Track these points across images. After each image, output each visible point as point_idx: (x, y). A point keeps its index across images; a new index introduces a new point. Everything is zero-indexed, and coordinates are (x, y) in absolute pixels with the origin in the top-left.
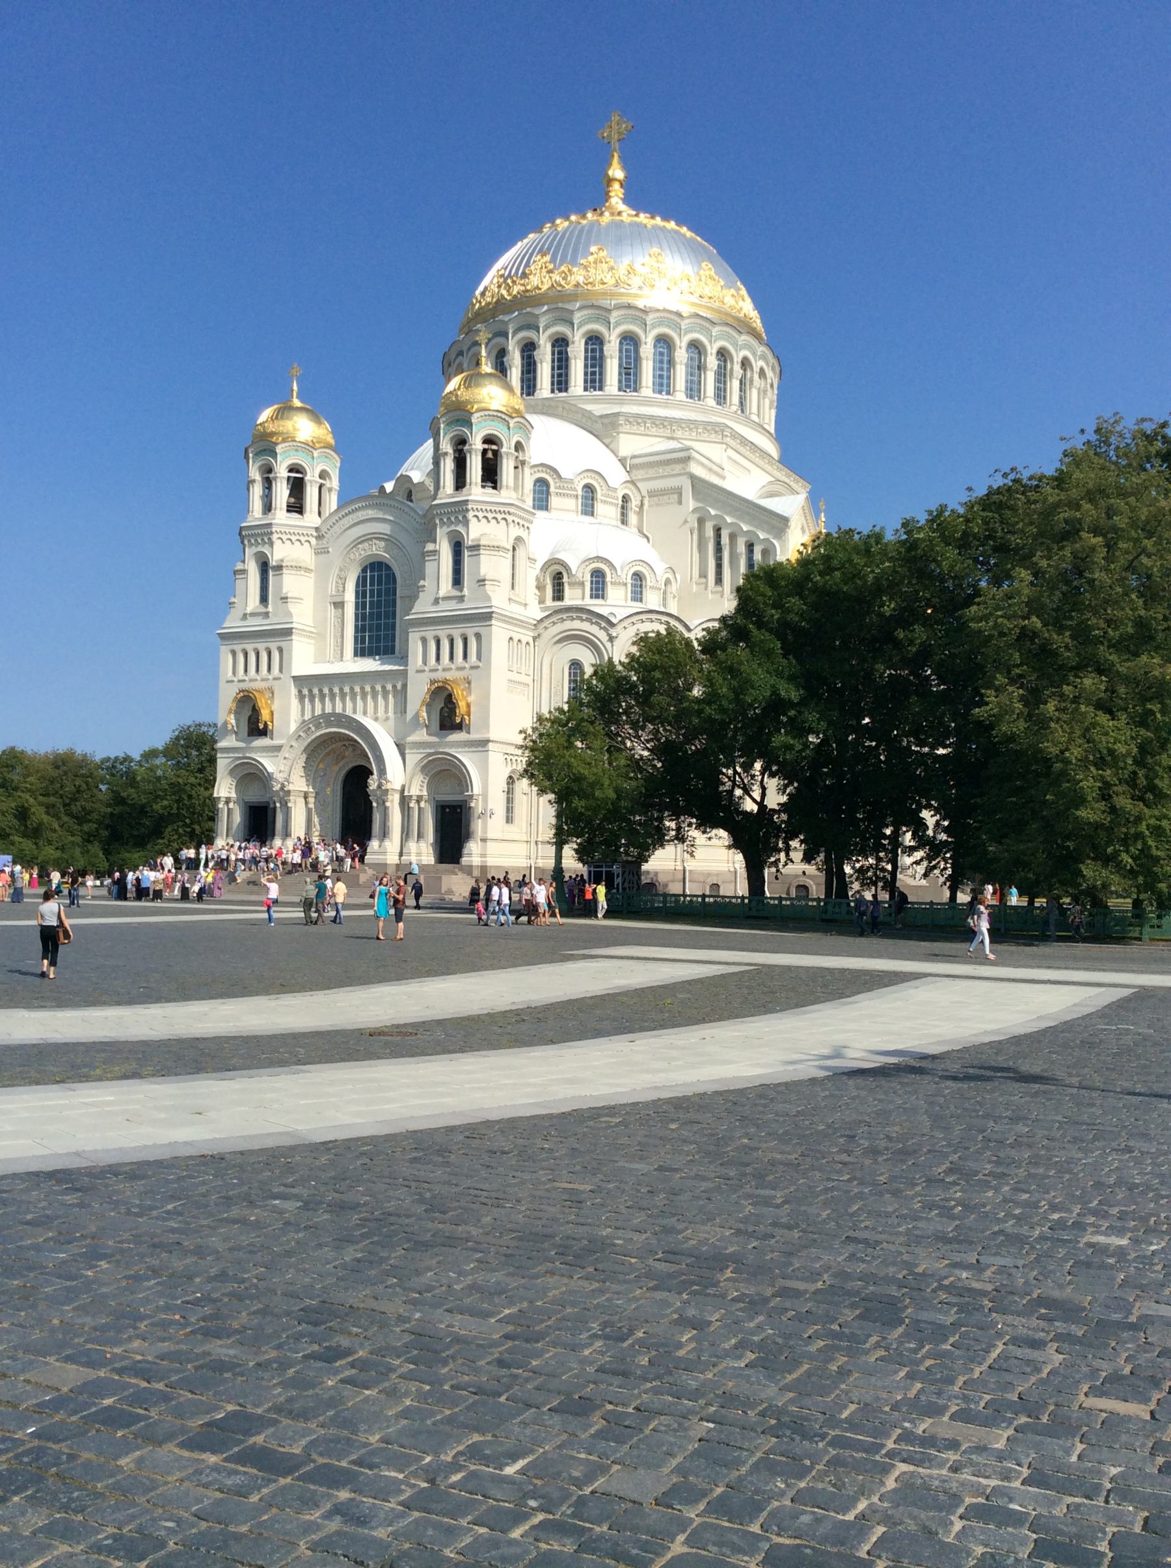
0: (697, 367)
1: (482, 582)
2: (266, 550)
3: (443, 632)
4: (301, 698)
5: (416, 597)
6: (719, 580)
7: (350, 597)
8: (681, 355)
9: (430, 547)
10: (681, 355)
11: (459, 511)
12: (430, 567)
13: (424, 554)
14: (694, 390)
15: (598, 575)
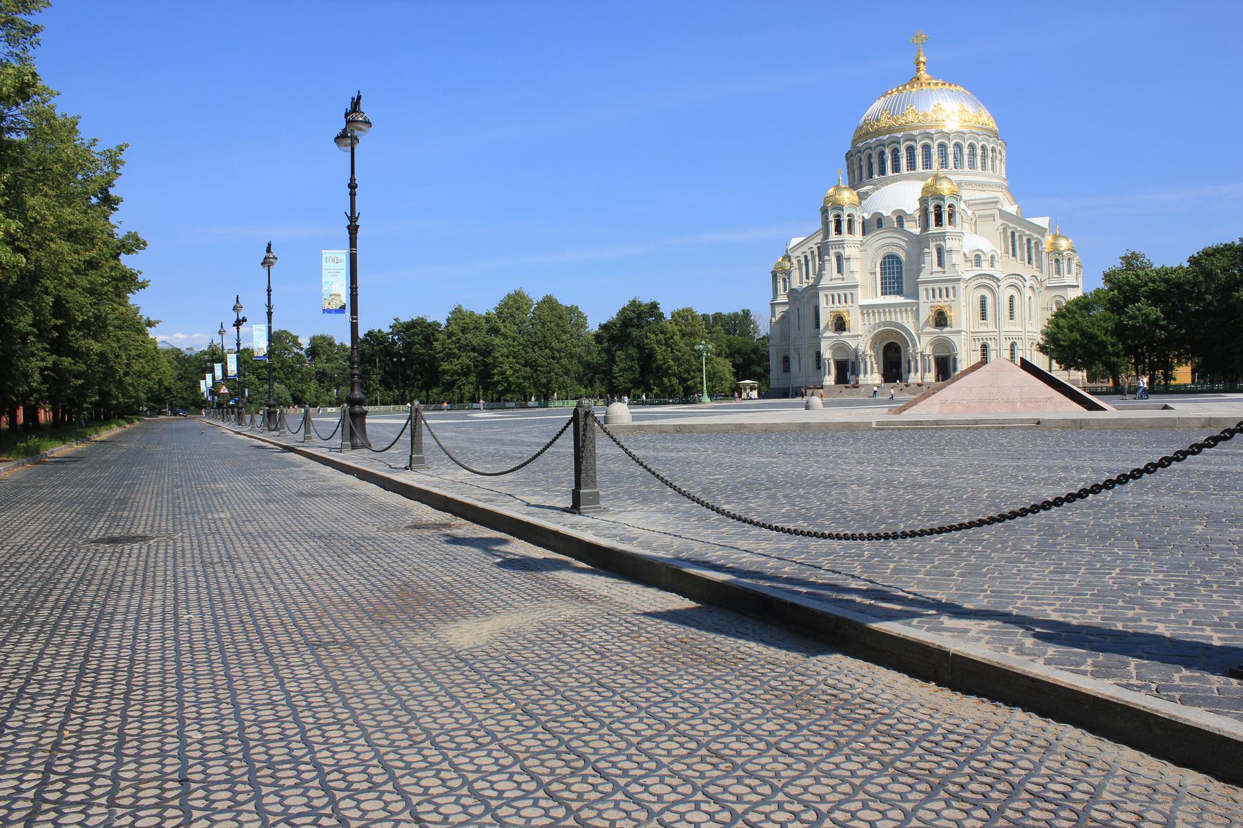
0: (984, 156)
1: (954, 265)
2: (841, 251)
3: (936, 286)
4: (863, 314)
5: (919, 272)
6: (1014, 255)
7: (878, 270)
8: (979, 152)
9: (926, 250)
10: (979, 152)
11: (942, 236)
12: (927, 259)
13: (923, 254)
14: (972, 165)
15: (978, 257)
